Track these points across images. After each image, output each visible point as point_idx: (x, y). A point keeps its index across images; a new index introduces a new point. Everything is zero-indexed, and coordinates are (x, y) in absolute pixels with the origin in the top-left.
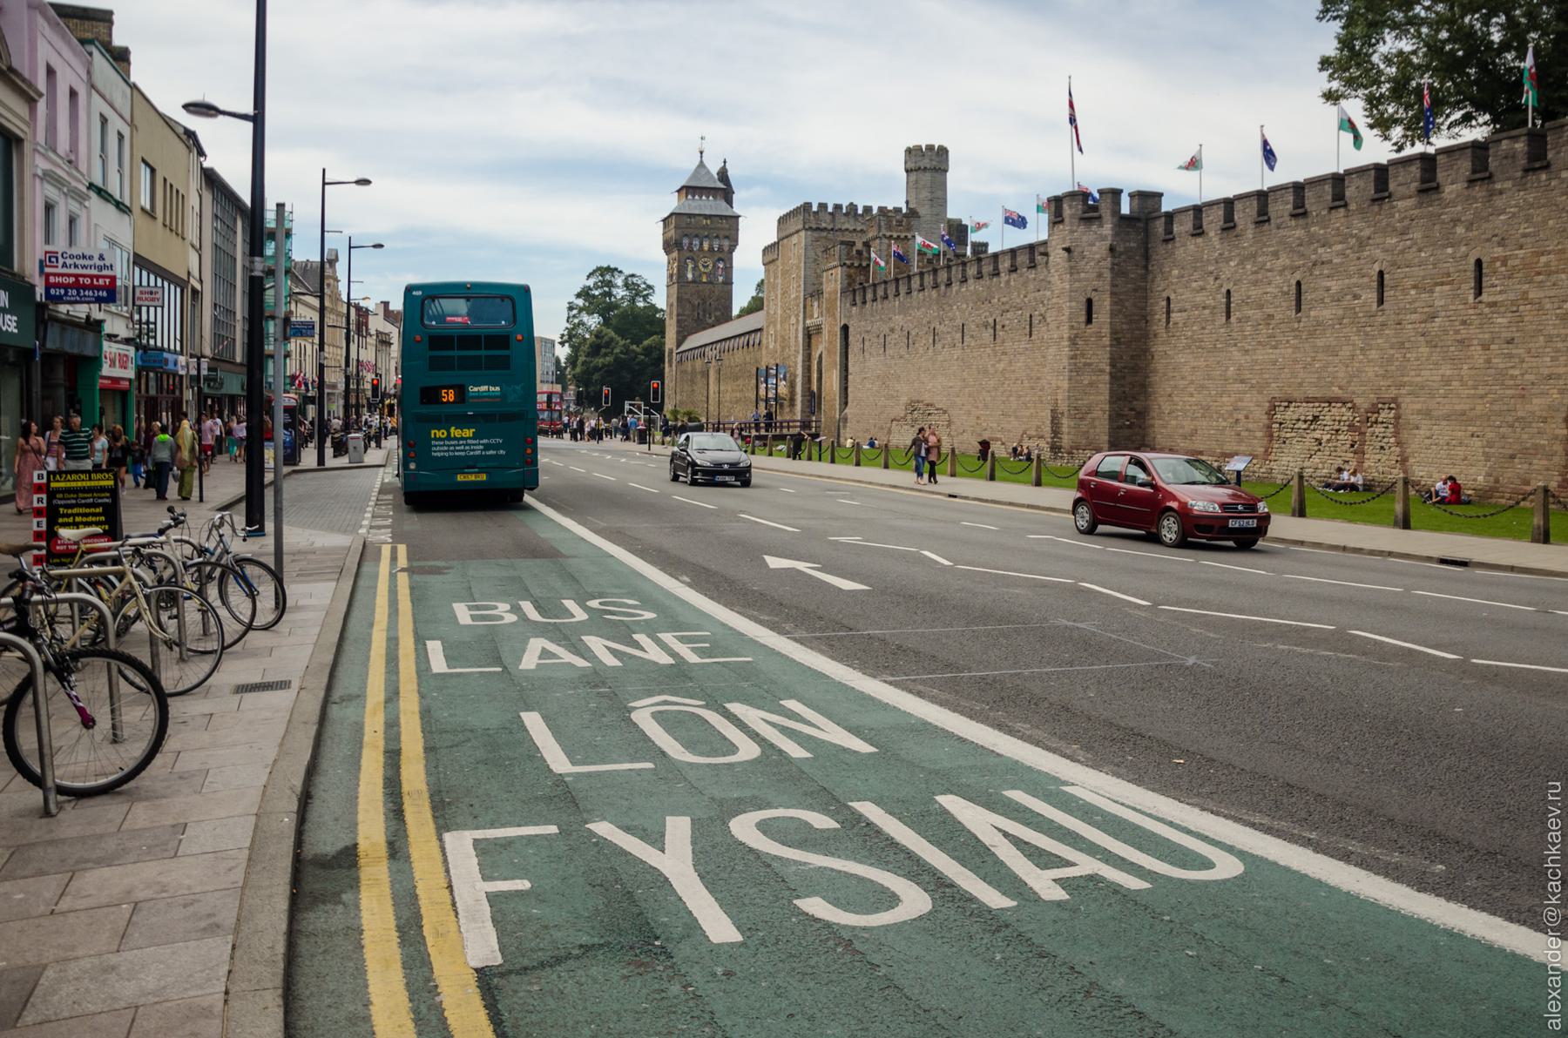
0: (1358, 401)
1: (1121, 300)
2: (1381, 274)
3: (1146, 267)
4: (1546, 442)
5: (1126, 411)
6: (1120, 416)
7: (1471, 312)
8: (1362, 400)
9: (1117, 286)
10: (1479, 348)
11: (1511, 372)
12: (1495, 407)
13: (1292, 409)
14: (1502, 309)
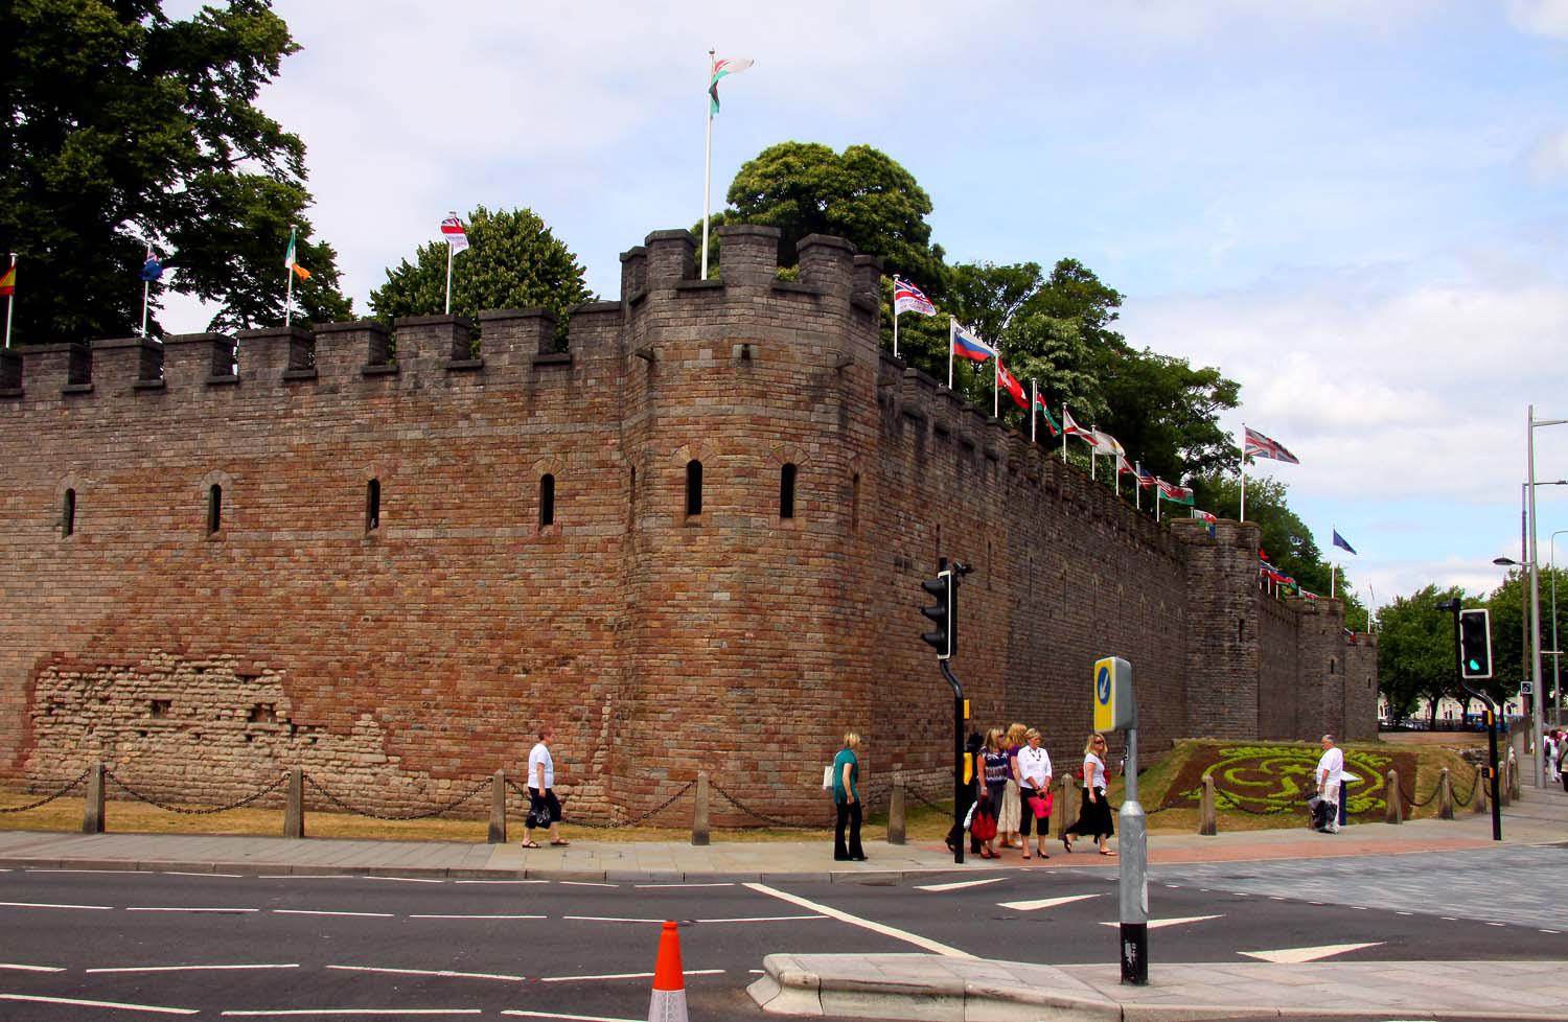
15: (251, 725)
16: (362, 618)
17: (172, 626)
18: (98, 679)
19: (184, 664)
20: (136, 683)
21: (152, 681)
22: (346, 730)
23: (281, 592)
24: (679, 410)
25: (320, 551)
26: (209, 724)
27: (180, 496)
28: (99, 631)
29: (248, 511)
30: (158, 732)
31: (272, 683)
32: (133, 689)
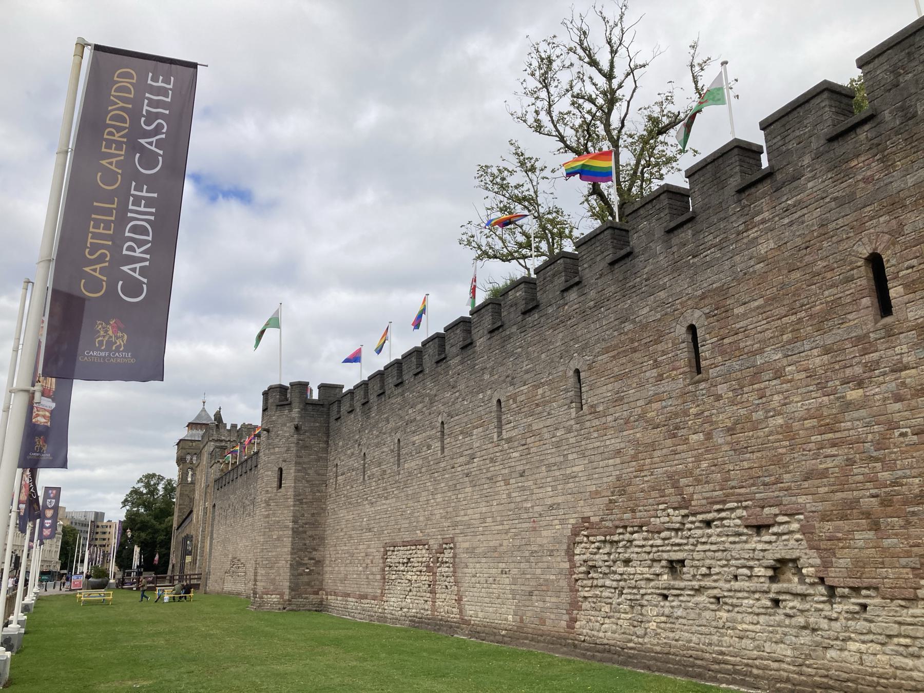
0: (431, 542)
1: (305, 468)
3: (327, 442)
4: (554, 577)
5: (306, 560)
6: (300, 564)
7: (496, 449)
9: (301, 457)
10: (502, 483)
11: (525, 505)
12: (517, 543)
14: (516, 444)
15: (775, 587)
16: (897, 433)
17: (673, 480)
18: (619, 541)
19: (691, 519)
20: (651, 542)
21: (664, 539)
22: (909, 593)
23: (780, 421)
25: (818, 361)
26: (727, 586)
27: (660, 347)
28: (613, 494)
29: (726, 341)
30: (678, 596)
31: (791, 532)
32: (648, 549)
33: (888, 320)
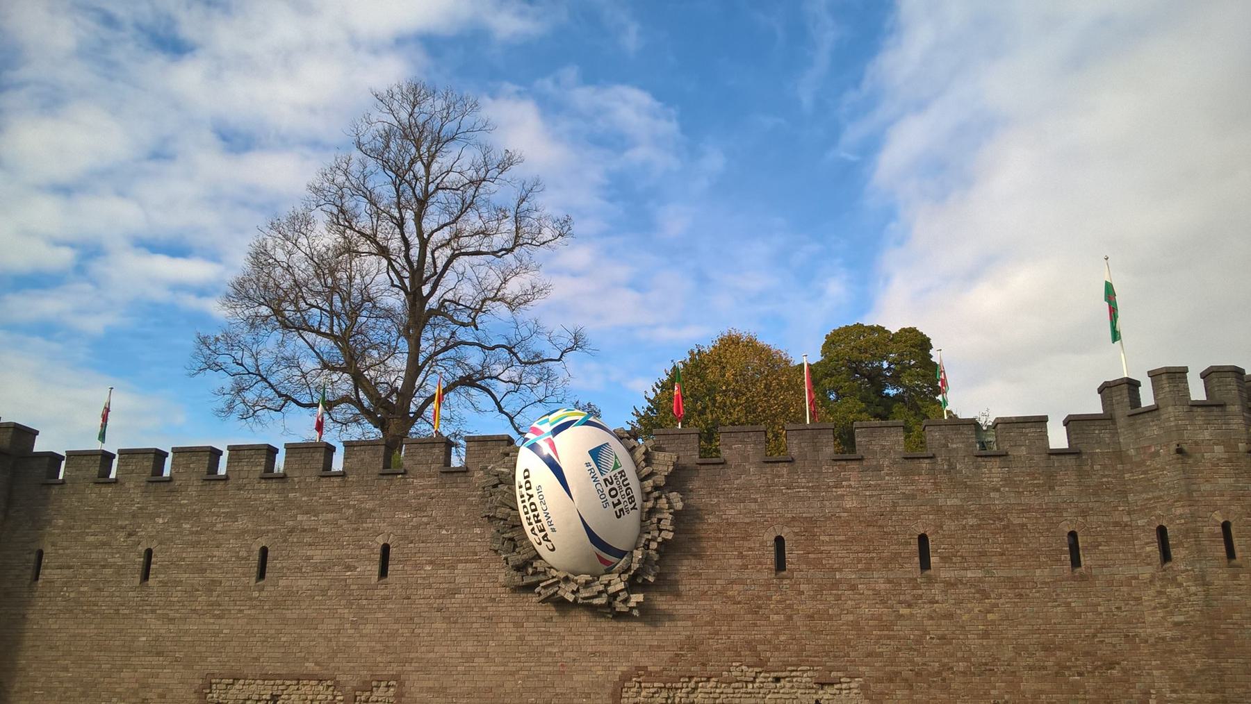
0: (342, 678)
2: (386, 549)
8: (349, 677)
10: (511, 625)
12: (529, 684)
13: (237, 686)
18: (682, 688)
21: (734, 688)
23: (851, 617)
24: (1208, 487)
25: (883, 586)
27: (746, 544)
33: (928, 572)
